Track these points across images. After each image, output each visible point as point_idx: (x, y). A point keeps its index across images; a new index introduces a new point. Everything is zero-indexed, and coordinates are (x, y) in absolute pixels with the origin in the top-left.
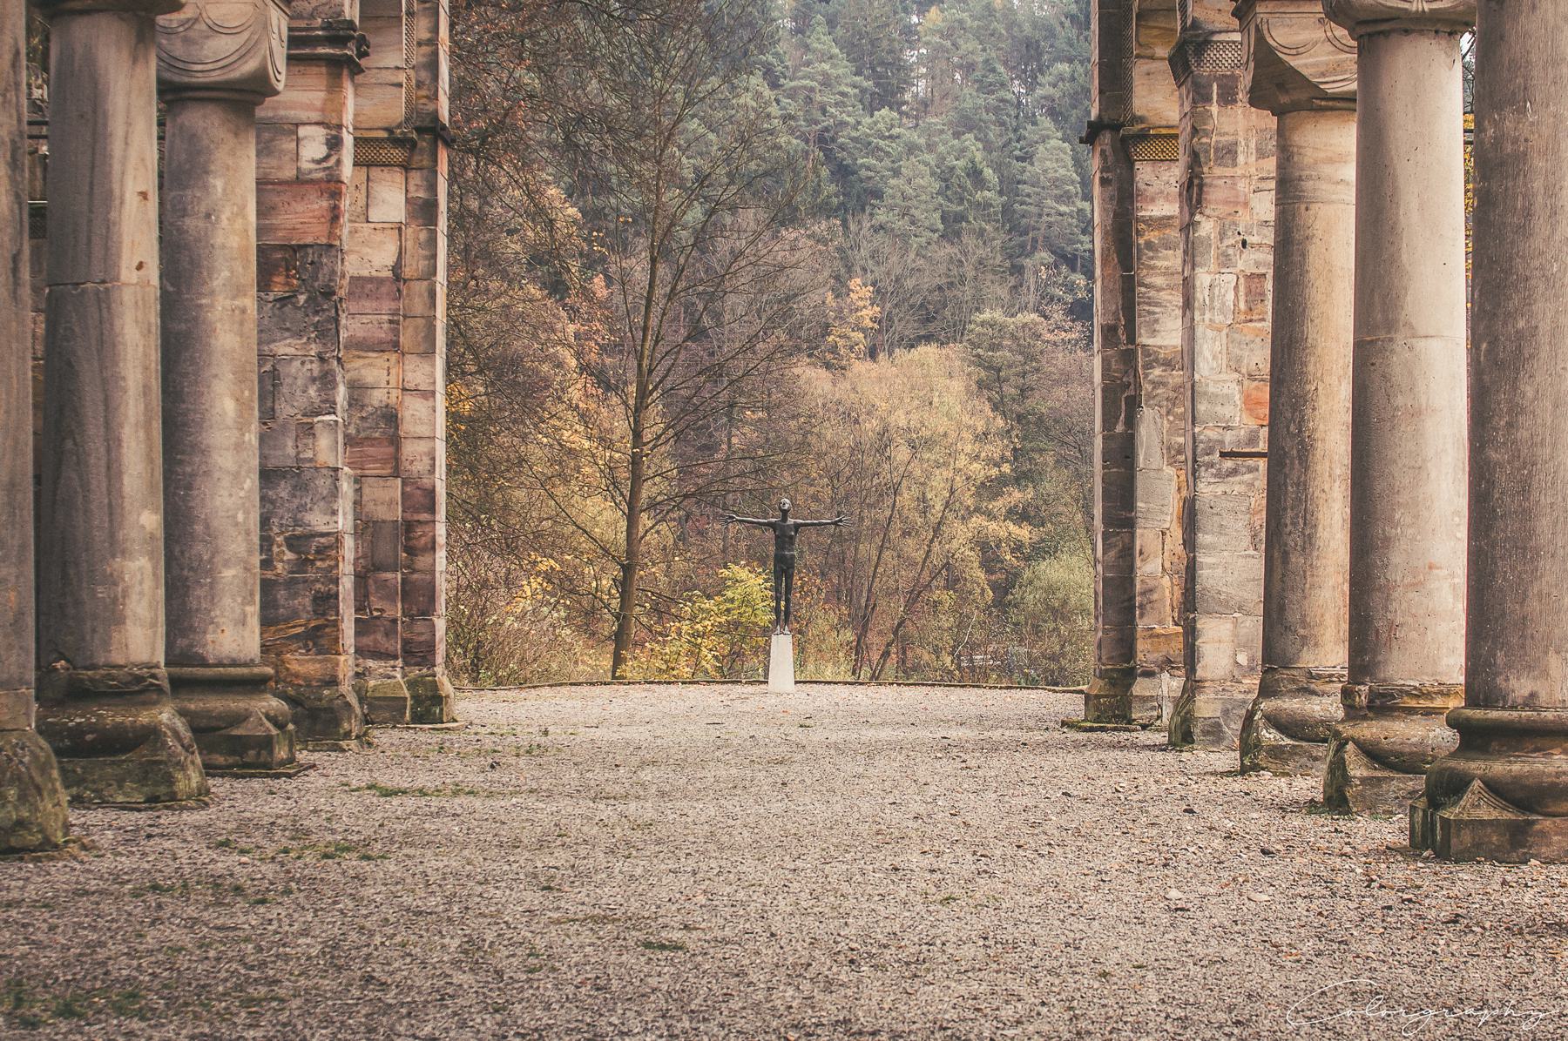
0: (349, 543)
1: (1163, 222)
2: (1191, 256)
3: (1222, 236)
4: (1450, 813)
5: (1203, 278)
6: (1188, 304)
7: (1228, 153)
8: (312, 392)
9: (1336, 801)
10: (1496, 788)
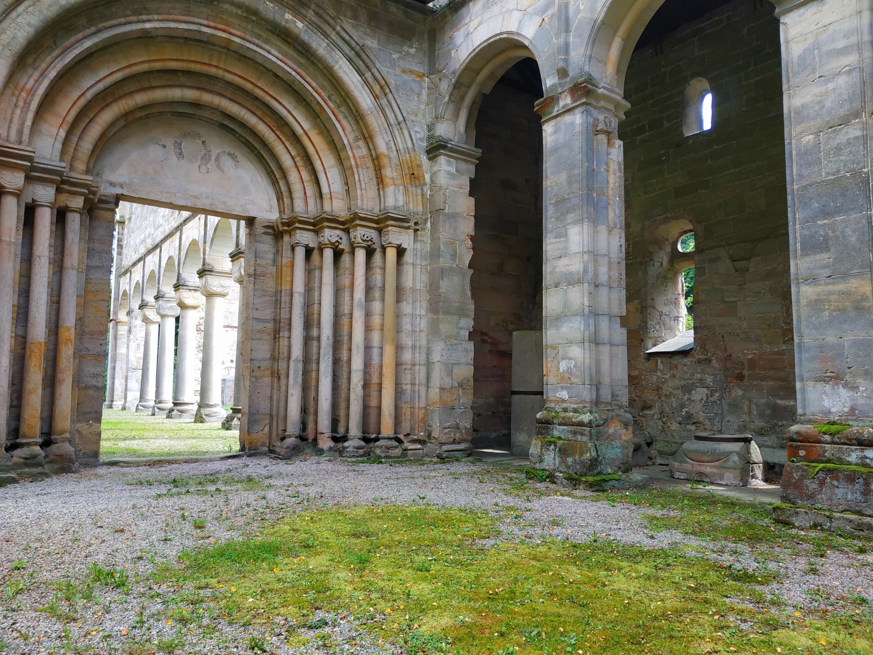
1: (123, 334)
2: (128, 340)
5: (131, 344)
6: (128, 347)
7: (135, 327)
9: (153, 414)
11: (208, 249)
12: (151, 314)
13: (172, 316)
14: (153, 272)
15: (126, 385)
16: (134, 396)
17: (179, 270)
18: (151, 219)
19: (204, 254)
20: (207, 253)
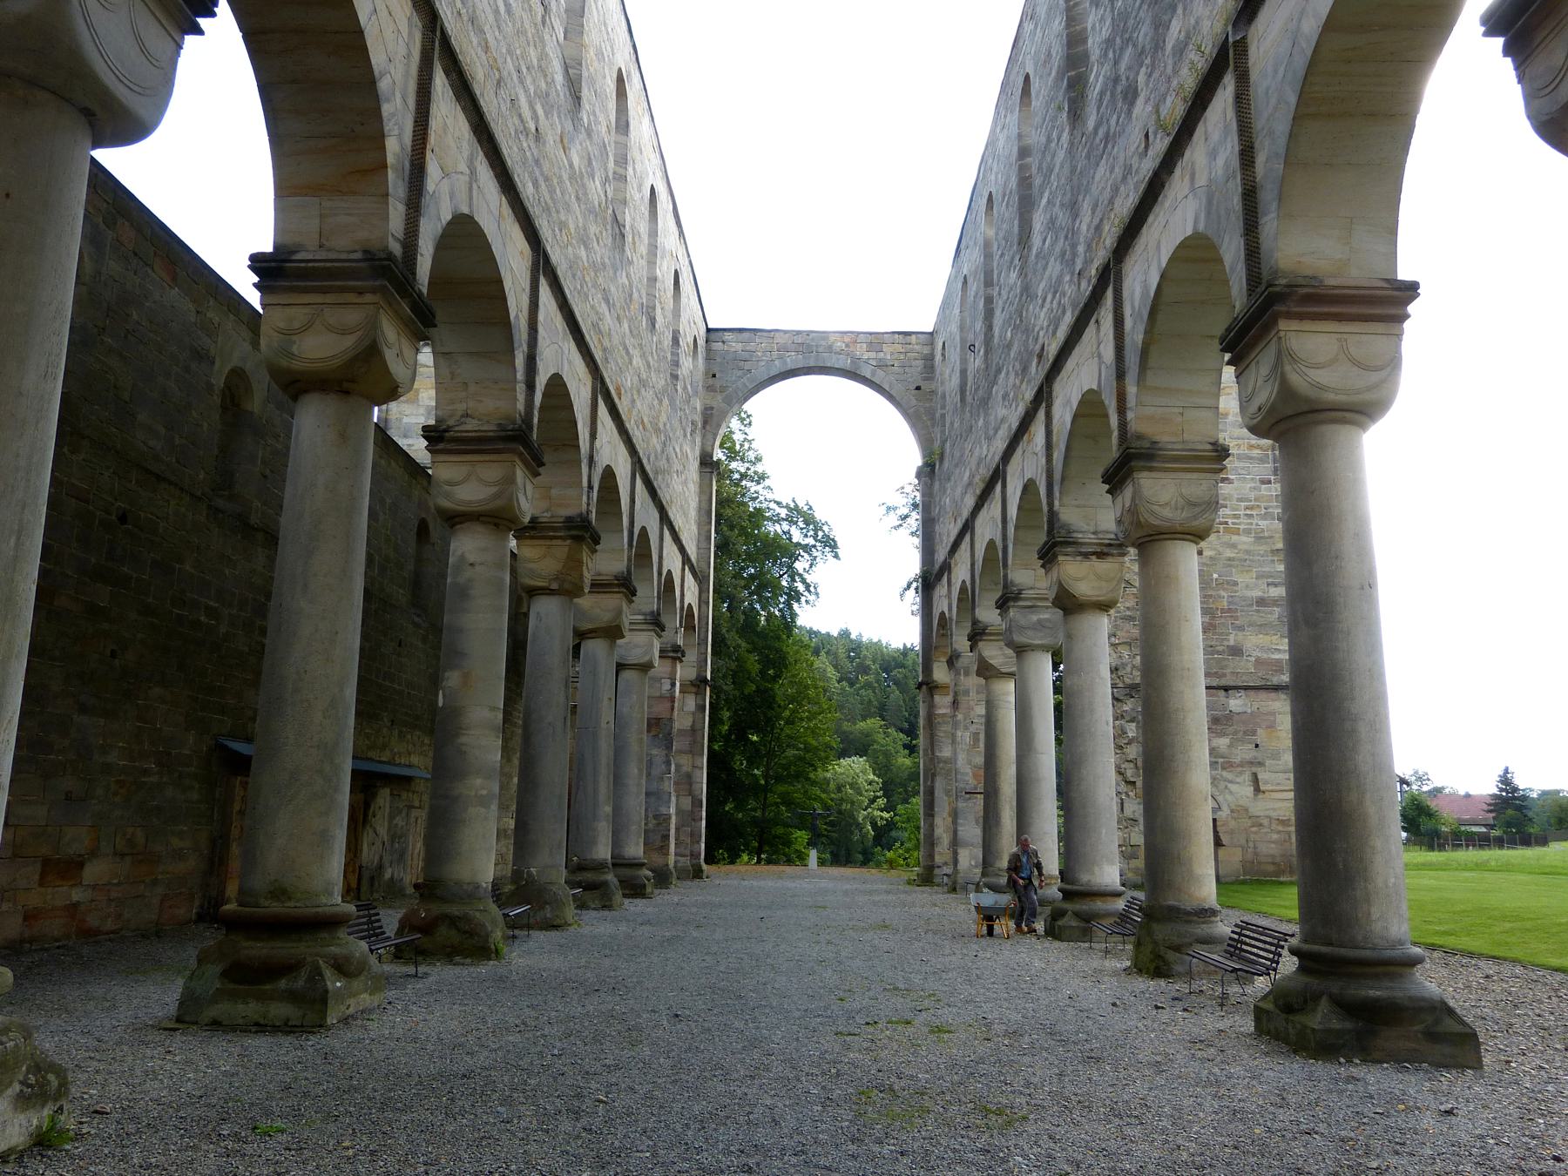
0: (673, 820)
3: (965, 720)
4: (1060, 923)
5: (959, 734)
6: (954, 742)
7: (967, 692)
8: (663, 767)
10: (1077, 915)
11: (1132, 390)
12: (995, 654)
13: (1044, 648)
14: (991, 544)
15: (955, 832)
16: (969, 859)
17: (1051, 504)
18: (981, 423)
19: (1122, 409)
20: (1131, 401)
